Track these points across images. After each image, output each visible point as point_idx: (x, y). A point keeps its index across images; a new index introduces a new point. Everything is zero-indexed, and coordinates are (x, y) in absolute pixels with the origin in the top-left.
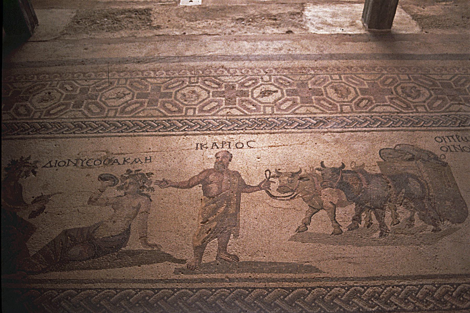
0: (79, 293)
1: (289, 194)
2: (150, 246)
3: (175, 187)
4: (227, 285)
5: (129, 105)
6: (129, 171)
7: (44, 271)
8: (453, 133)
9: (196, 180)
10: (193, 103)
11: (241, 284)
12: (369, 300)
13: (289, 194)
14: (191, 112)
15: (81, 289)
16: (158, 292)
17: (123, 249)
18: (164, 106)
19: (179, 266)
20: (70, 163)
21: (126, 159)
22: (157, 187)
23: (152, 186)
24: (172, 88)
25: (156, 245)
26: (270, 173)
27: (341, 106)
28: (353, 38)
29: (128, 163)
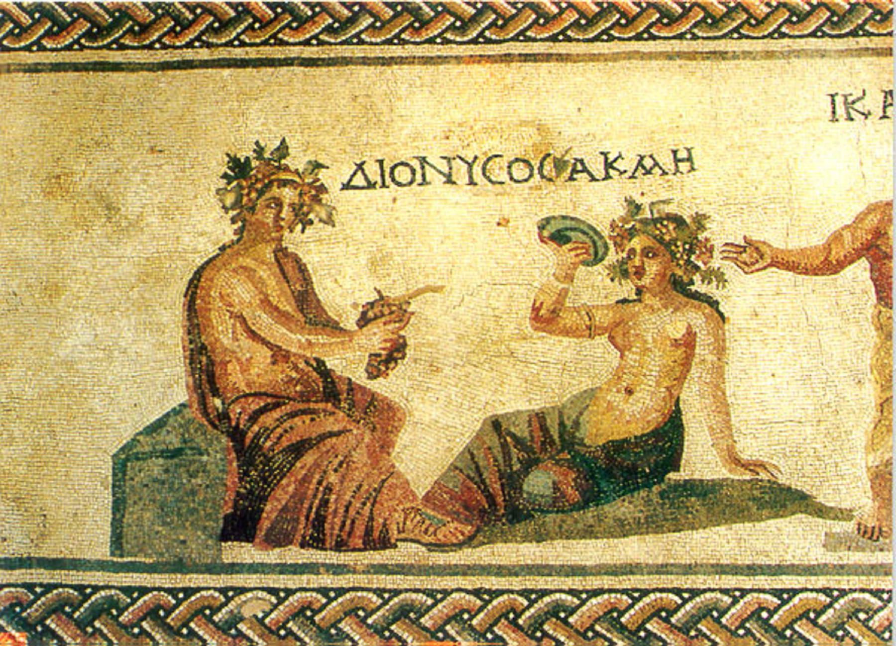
0: (583, 602)
2: (746, 466)
7: (469, 541)
15: (587, 592)
16: (790, 599)
20: (430, 173)
21: (611, 158)
22: (730, 270)
25: (762, 465)
29: (622, 173)
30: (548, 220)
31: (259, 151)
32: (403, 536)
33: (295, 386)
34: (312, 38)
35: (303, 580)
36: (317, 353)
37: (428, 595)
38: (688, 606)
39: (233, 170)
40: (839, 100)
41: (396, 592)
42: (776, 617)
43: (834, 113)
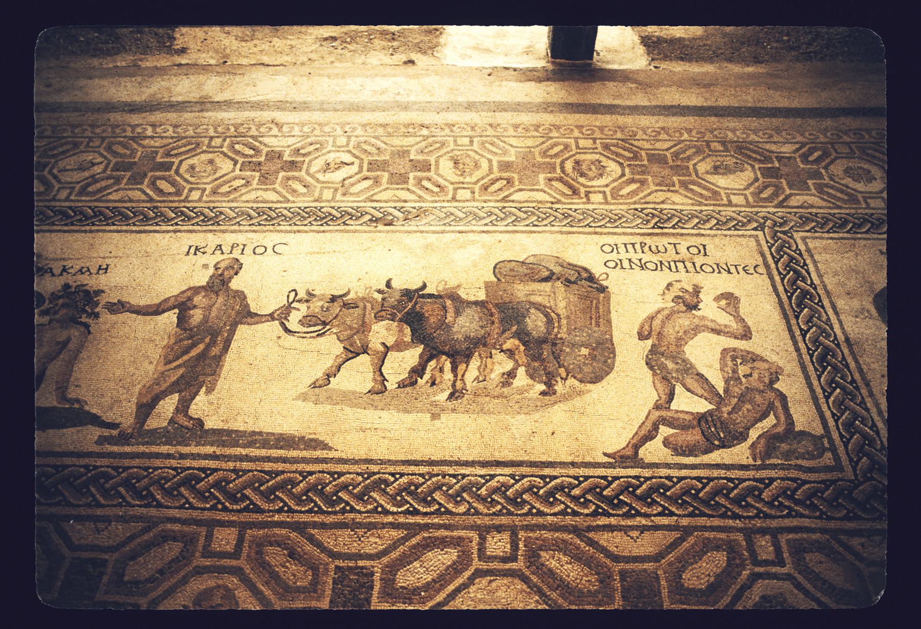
1: (316, 328)
4: (174, 463)
5: (96, 181)
6: (67, 286)
8: (638, 240)
9: (170, 303)
10: (205, 181)
11: (196, 464)
12: (398, 494)
13: (316, 328)
14: (195, 195)
18: (153, 184)
19: (106, 432)
23: (97, 310)
24: (176, 155)
25: (78, 401)
26: (296, 295)
27: (456, 189)
28: (529, 75)
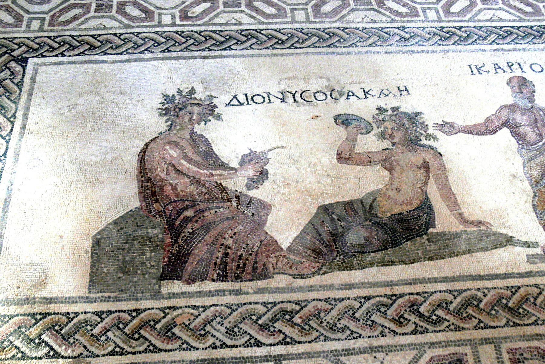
3: (470, 132)
15: (395, 295)
17: (431, 230)
19: (532, 251)
22: (439, 134)
23: (430, 131)
30: (338, 116)
31: (180, 92)
32: (276, 271)
33: (205, 195)
34: (206, 48)
35: (214, 300)
36: (216, 178)
37: (296, 304)
38: (459, 299)
39: (165, 100)
40: (473, 67)
41: (275, 304)
42: (511, 302)
43: (472, 71)
